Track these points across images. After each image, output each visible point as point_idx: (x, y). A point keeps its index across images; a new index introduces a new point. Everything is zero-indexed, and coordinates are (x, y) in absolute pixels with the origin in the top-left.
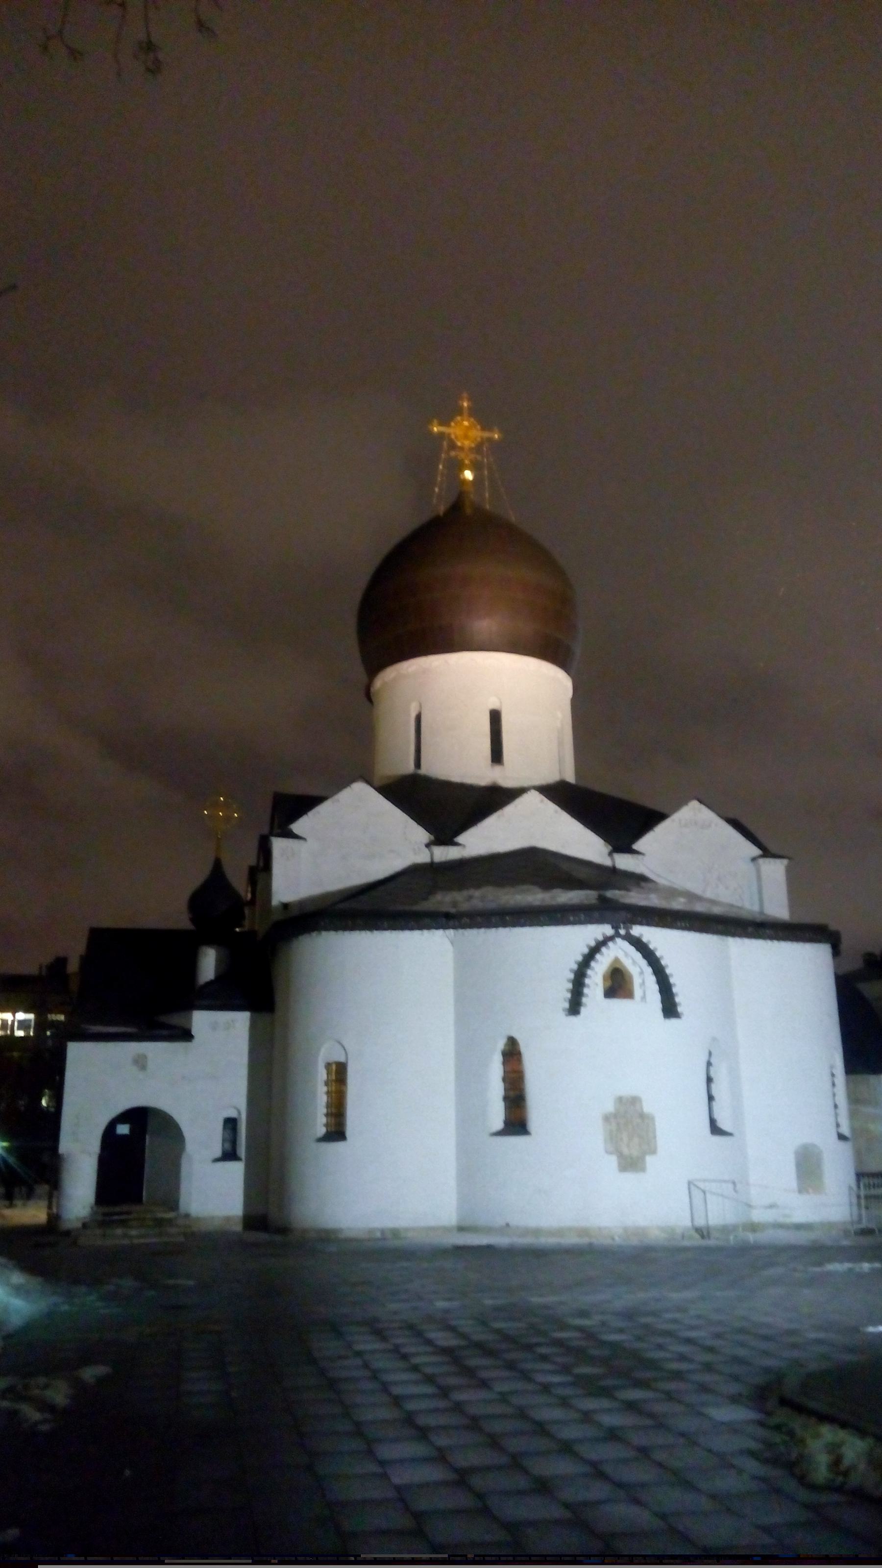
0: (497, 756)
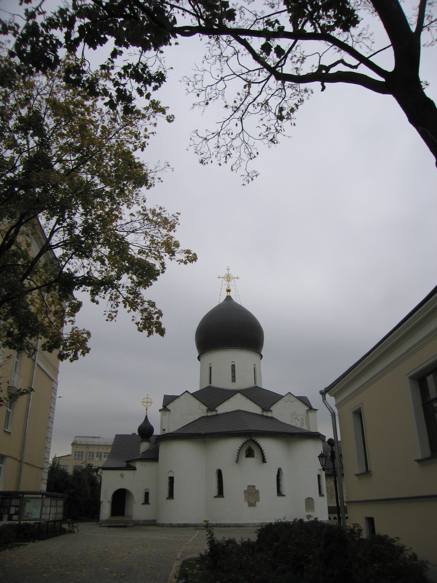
0: (234, 379)
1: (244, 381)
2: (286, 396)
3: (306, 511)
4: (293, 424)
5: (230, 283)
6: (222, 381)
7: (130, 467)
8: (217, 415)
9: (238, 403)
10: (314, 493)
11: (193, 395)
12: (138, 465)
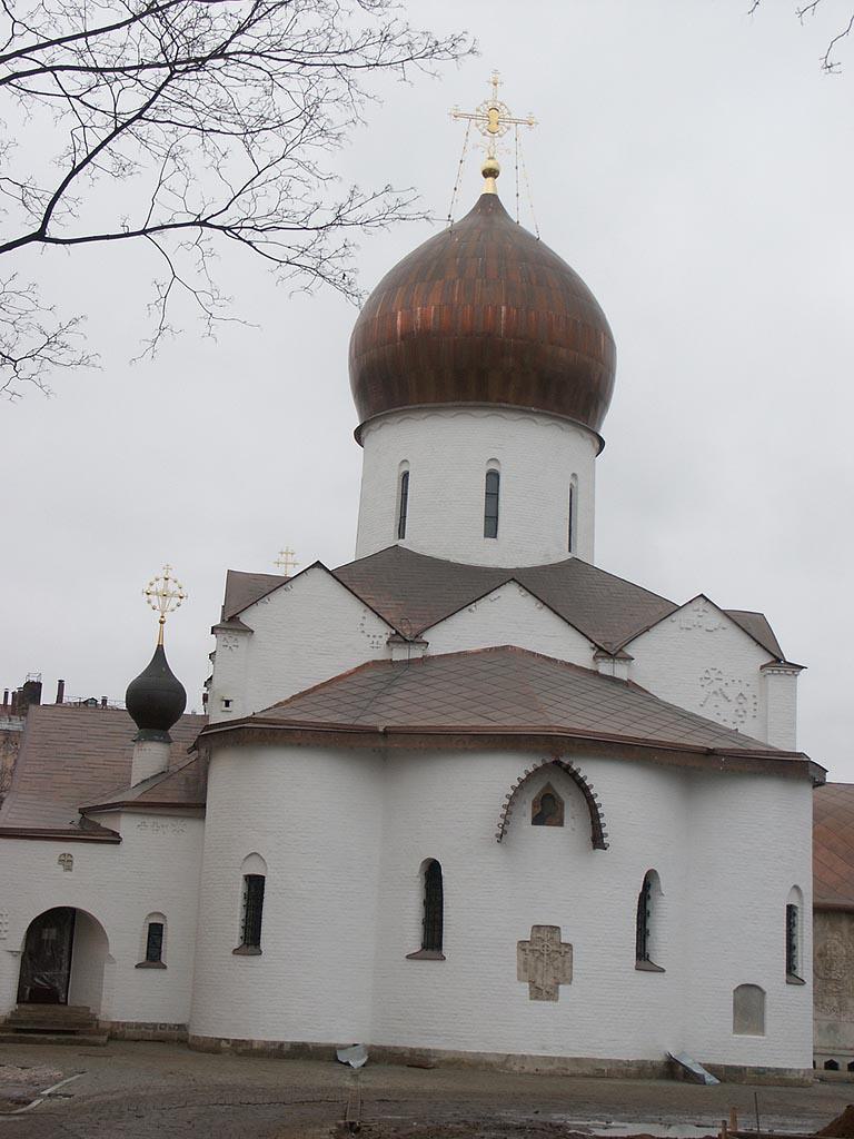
1: (528, 541)
2: (689, 607)
3: (738, 1028)
4: (708, 714)
6: (448, 533)
7: (92, 828)
8: (425, 660)
9: (508, 622)
10: (769, 973)
11: (343, 577)
12: (126, 825)
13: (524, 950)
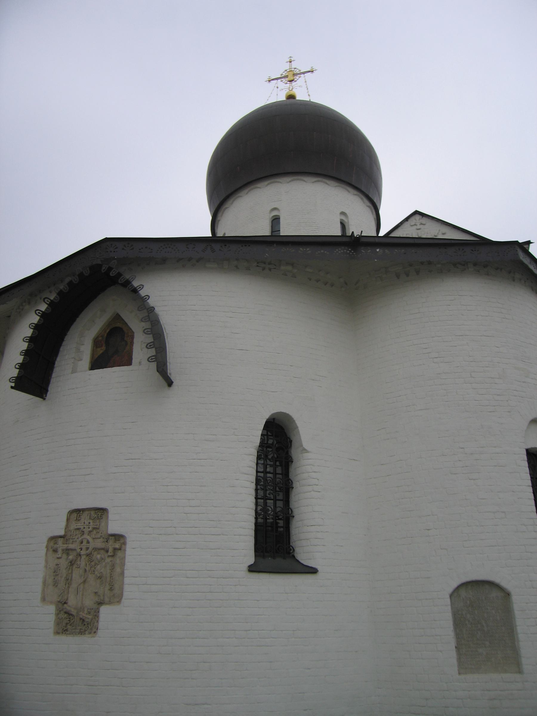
5: (294, 83)
13: (55, 551)
